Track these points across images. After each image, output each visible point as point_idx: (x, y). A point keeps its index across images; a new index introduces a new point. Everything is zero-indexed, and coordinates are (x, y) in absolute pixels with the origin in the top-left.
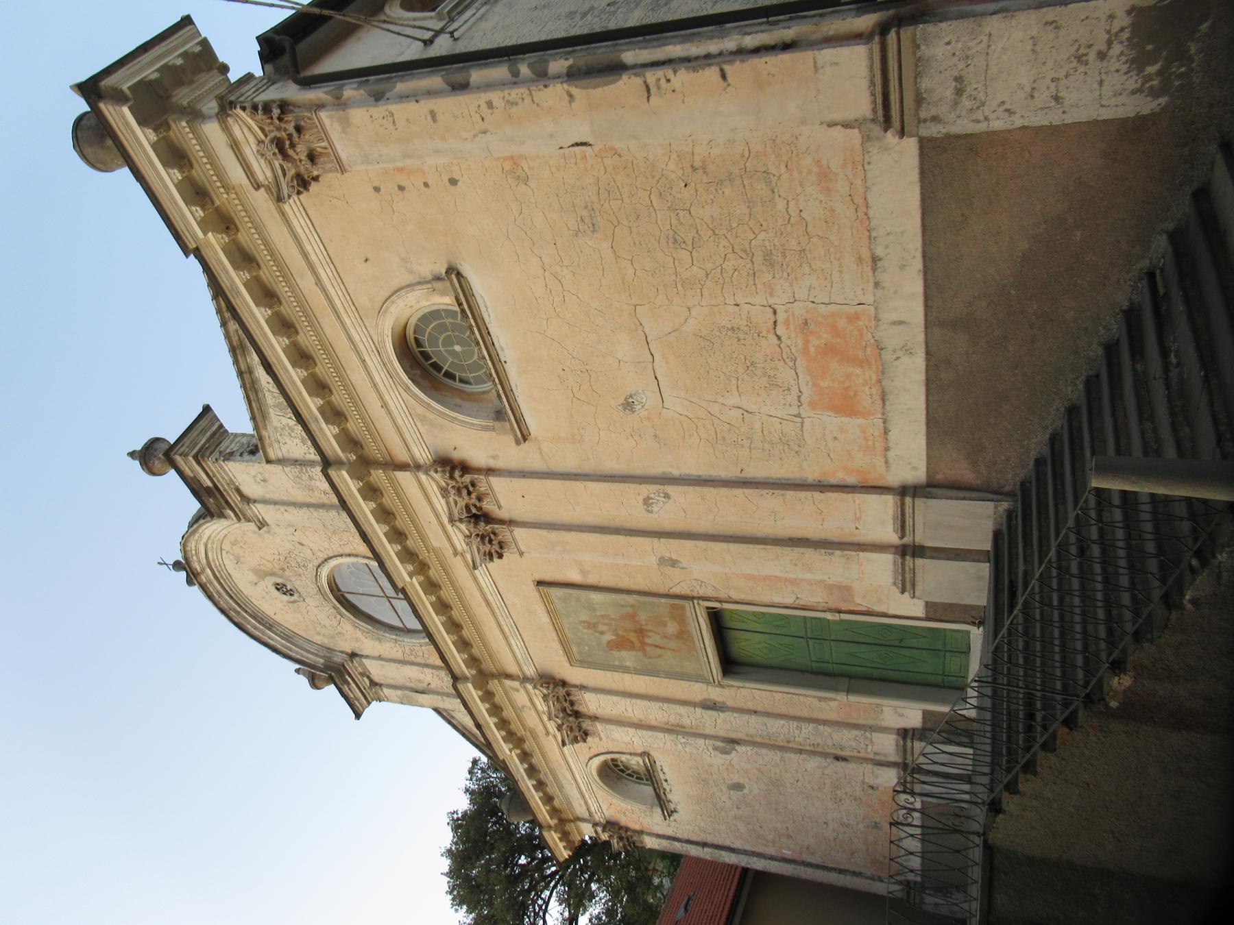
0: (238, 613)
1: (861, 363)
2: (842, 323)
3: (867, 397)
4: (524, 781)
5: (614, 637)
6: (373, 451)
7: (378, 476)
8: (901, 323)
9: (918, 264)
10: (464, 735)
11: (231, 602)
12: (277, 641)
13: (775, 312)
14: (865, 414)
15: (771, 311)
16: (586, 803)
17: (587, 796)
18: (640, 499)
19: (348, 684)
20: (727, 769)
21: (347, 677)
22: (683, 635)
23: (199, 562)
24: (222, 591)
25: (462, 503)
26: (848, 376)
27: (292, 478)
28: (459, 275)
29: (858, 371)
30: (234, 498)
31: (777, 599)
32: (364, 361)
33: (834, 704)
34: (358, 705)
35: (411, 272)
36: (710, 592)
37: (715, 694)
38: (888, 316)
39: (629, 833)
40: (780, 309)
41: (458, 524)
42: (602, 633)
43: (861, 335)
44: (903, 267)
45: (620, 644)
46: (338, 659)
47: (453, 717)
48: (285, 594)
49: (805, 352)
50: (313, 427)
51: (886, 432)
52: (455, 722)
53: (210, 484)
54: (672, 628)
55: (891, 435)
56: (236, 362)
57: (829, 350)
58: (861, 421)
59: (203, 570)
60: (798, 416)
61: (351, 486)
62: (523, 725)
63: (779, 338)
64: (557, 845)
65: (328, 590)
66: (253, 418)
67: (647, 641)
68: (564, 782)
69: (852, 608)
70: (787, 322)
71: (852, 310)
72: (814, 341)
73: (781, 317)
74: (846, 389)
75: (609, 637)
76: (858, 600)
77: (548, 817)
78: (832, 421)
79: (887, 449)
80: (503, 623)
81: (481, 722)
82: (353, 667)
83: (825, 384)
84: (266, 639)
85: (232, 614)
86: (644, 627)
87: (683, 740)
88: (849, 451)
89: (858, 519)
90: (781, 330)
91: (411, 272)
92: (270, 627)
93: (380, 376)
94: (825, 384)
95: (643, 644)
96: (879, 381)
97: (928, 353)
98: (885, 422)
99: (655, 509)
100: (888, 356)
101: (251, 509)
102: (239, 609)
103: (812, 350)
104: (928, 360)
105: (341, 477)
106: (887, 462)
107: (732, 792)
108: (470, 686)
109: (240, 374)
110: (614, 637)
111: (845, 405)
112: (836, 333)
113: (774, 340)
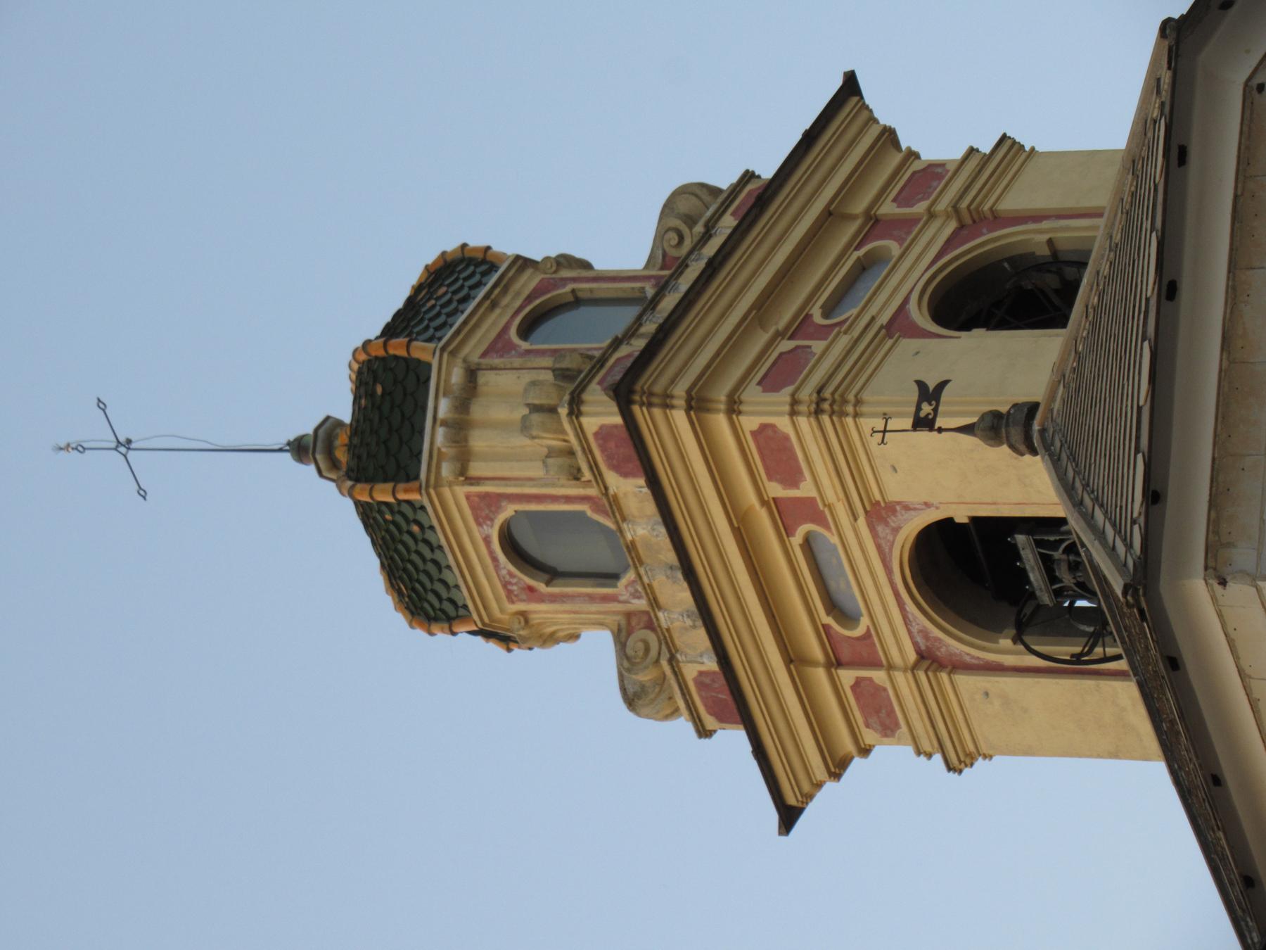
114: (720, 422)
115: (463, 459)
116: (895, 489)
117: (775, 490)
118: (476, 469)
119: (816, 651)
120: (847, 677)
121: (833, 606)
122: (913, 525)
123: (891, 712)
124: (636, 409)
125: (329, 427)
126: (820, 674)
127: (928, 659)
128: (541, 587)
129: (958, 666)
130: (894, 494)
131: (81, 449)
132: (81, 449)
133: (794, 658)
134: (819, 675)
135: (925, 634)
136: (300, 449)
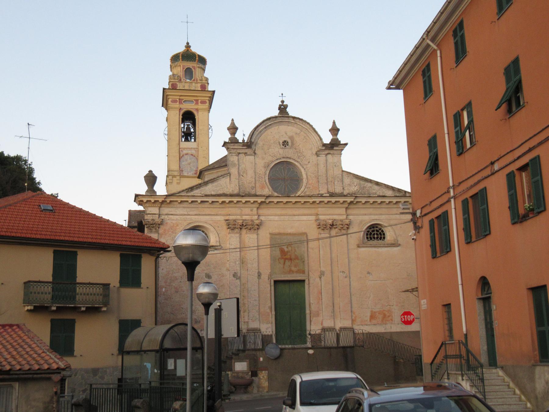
0: (274, 121)
1: (382, 321)
2: (390, 318)
3: (374, 321)
4: (201, 199)
5: (286, 251)
6: (351, 206)
7: (346, 205)
8: (391, 328)
9: (402, 331)
10: (214, 179)
11: (279, 121)
12: (261, 128)
13: (392, 306)
14: (370, 321)
15: (393, 305)
16: (177, 215)
17: (181, 217)
18: (344, 271)
19: (242, 146)
20: (220, 274)
21: (246, 147)
22: (291, 271)
23: (299, 122)
24: (283, 121)
25: (338, 224)
26: (379, 318)
27: (338, 175)
28: (398, 246)
29: (380, 320)
30: (326, 152)
31: (311, 299)
32: (377, 215)
33: (269, 311)
34: (231, 145)
35: (399, 236)
36: (311, 281)
37: (265, 277)
38: (392, 326)
39: (157, 228)
40: (393, 307)
41: (332, 221)
42: (287, 248)
43: (388, 321)
44: (402, 328)
45: (282, 252)
46: (253, 147)
47: (223, 177)
48: (283, 143)
49: (384, 311)
50: (366, 198)
51: (367, 325)
52: (221, 177)
53: (334, 149)
54: (293, 268)
55: (365, 326)
56: (375, 181)
57: (385, 316)
58: (369, 320)
59: (294, 121)
60: (369, 308)
61: (349, 200)
62: (231, 207)
63: (387, 306)
64: (154, 198)
65: (288, 160)
66: (358, 175)
67: (287, 261)
68: (188, 210)
69: (311, 317)
70: (390, 308)
71: (393, 319)
72: (386, 313)
73: (392, 307)
74: (376, 318)
75: (286, 250)
76: (314, 318)
77: (172, 200)
78: (369, 314)
79: (362, 325)
80: (287, 217)
81: (244, 197)
82: (249, 151)
83: (377, 314)
84: (262, 124)
85: (274, 119)
86: (293, 261)
87: (237, 263)
88: (361, 318)
89: (344, 319)
90: (388, 306)
91: (399, 236)
92: (265, 128)
93: (373, 217)
94: (377, 314)
95: (285, 259)
96: (378, 324)
97: (385, 333)
98: (369, 325)
99: (341, 273)
100: (384, 325)
101: (324, 155)
102: (275, 122)
103: (385, 312)
104: (384, 332)
105: (353, 199)
106: (359, 325)
107: (204, 274)
108: (264, 200)
109: (371, 180)
110: (286, 251)
111: (372, 317)
112: (389, 316)
113: (386, 305)
114: (208, 99)
115: (199, 67)
116: (200, 113)
117: (199, 101)
118: (198, 68)
119: (181, 98)
120: (178, 100)
121: (185, 101)
122: (195, 113)
123: (173, 103)
124: (212, 92)
125: (190, 47)
126: (179, 97)
127: (180, 109)
128: (184, 70)
129: (180, 112)
130: (199, 112)
131: (187, 17)
132: (187, 17)
133: (181, 96)
134: (179, 97)
135: (183, 109)
136: (188, 43)
